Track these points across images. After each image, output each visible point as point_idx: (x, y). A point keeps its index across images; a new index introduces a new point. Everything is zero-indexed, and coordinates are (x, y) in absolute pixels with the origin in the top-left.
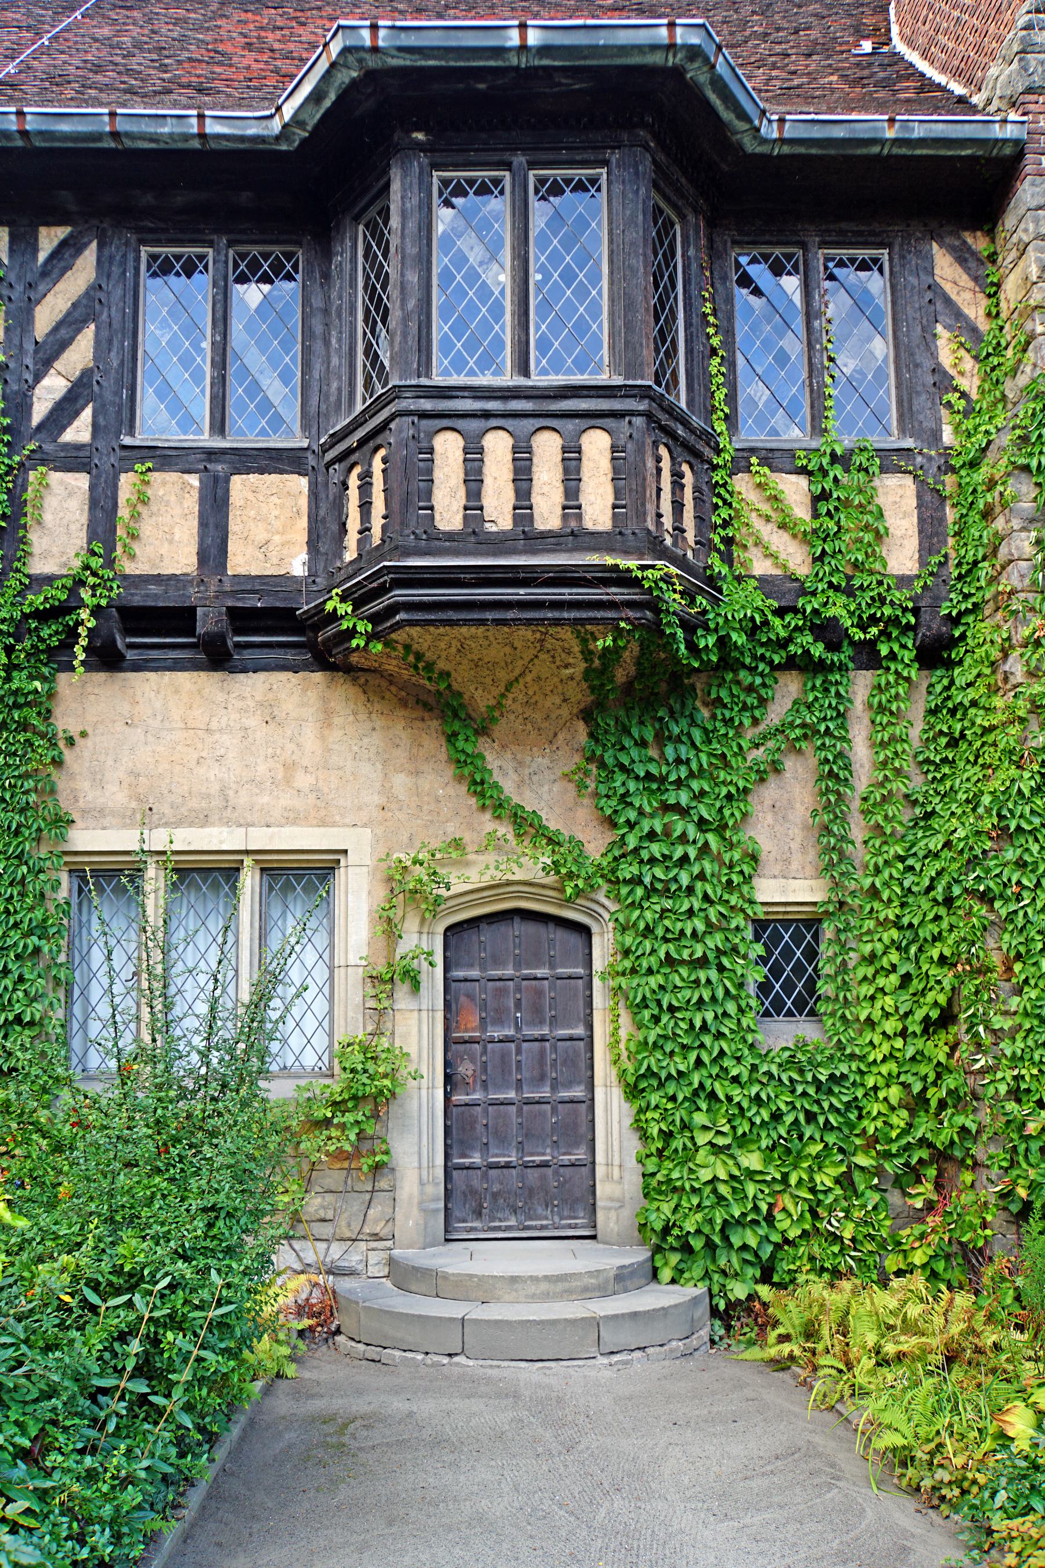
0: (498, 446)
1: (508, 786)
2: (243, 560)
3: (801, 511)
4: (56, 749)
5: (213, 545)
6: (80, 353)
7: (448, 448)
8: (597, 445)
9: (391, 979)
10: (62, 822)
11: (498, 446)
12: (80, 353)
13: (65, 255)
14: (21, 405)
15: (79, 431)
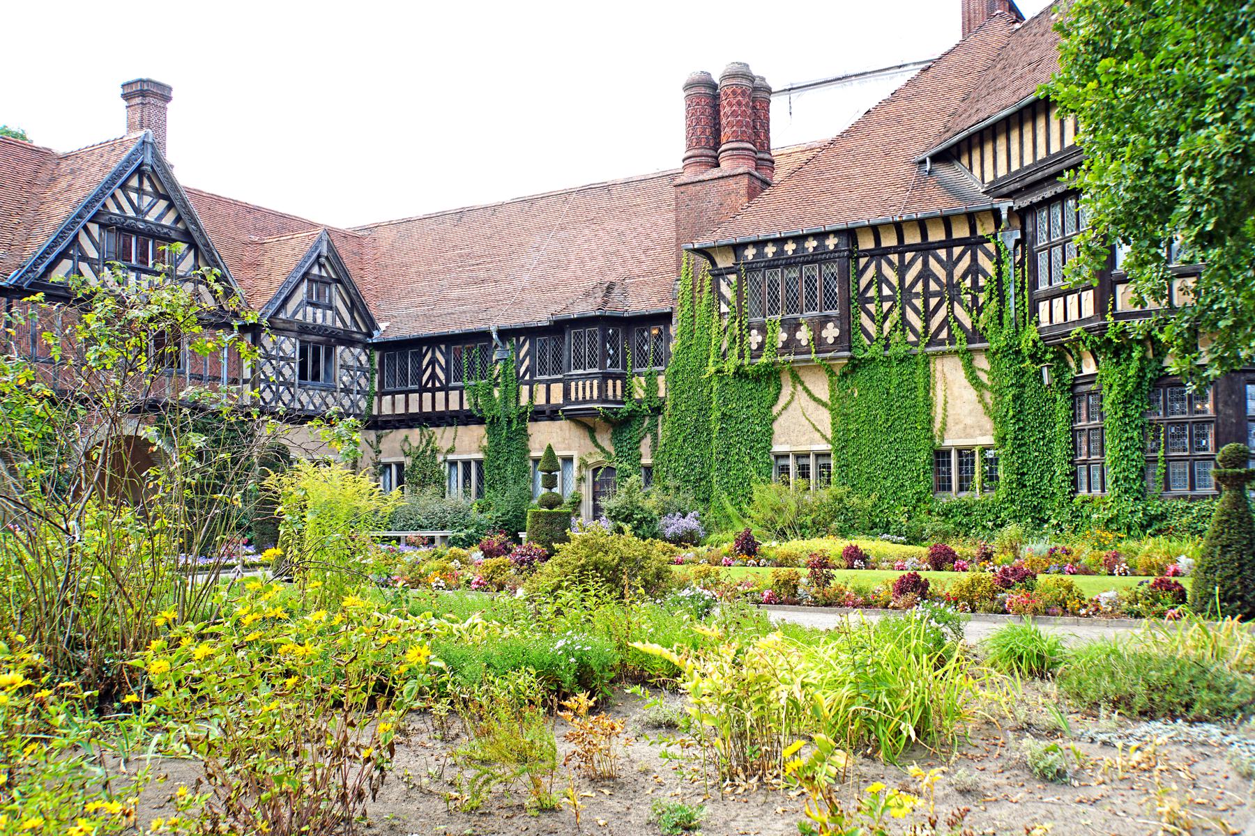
0: (580, 383)
1: (599, 441)
2: (553, 401)
3: (644, 384)
4: (527, 436)
5: (548, 400)
6: (527, 362)
7: (573, 384)
8: (595, 382)
9: (581, 479)
10: (529, 451)
11: (580, 383)
12: (527, 362)
13: (525, 341)
14: (518, 373)
15: (527, 377)
